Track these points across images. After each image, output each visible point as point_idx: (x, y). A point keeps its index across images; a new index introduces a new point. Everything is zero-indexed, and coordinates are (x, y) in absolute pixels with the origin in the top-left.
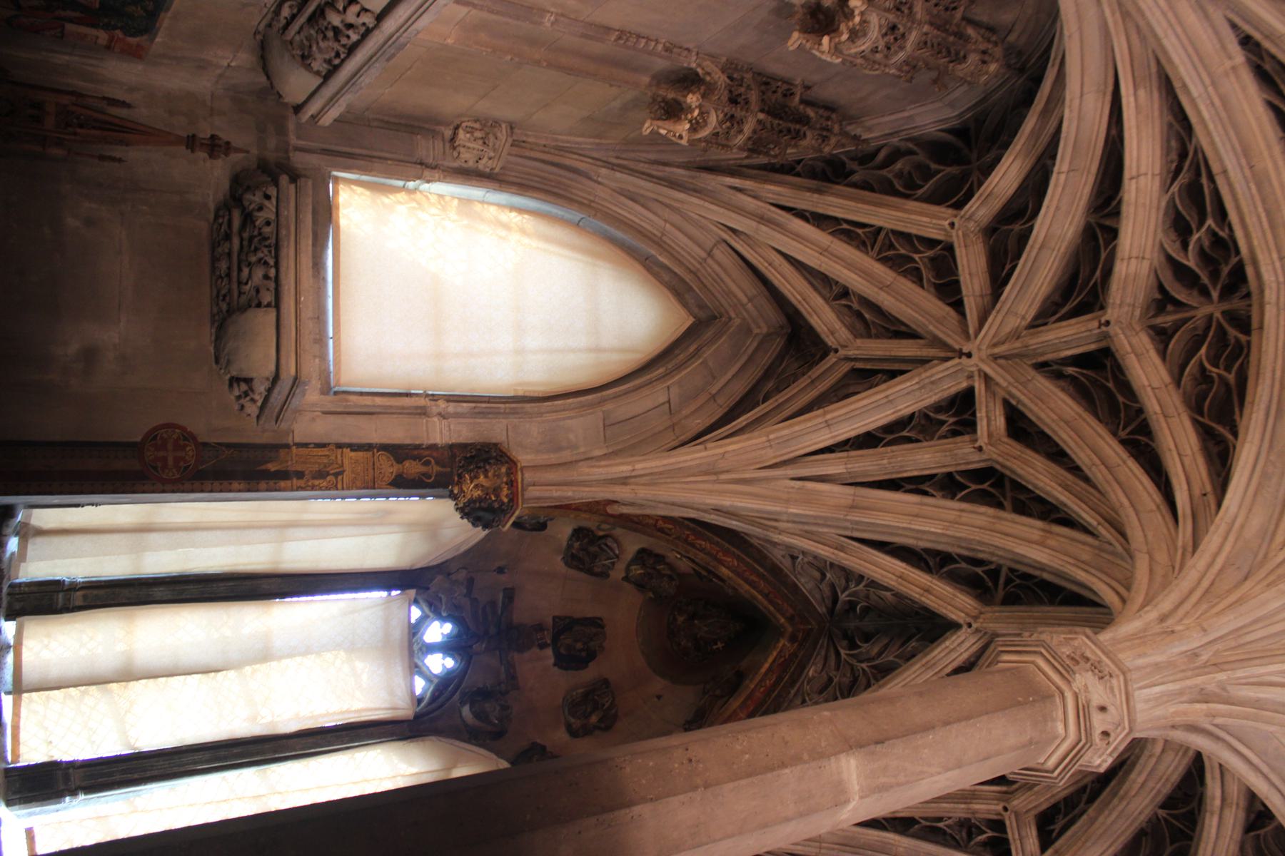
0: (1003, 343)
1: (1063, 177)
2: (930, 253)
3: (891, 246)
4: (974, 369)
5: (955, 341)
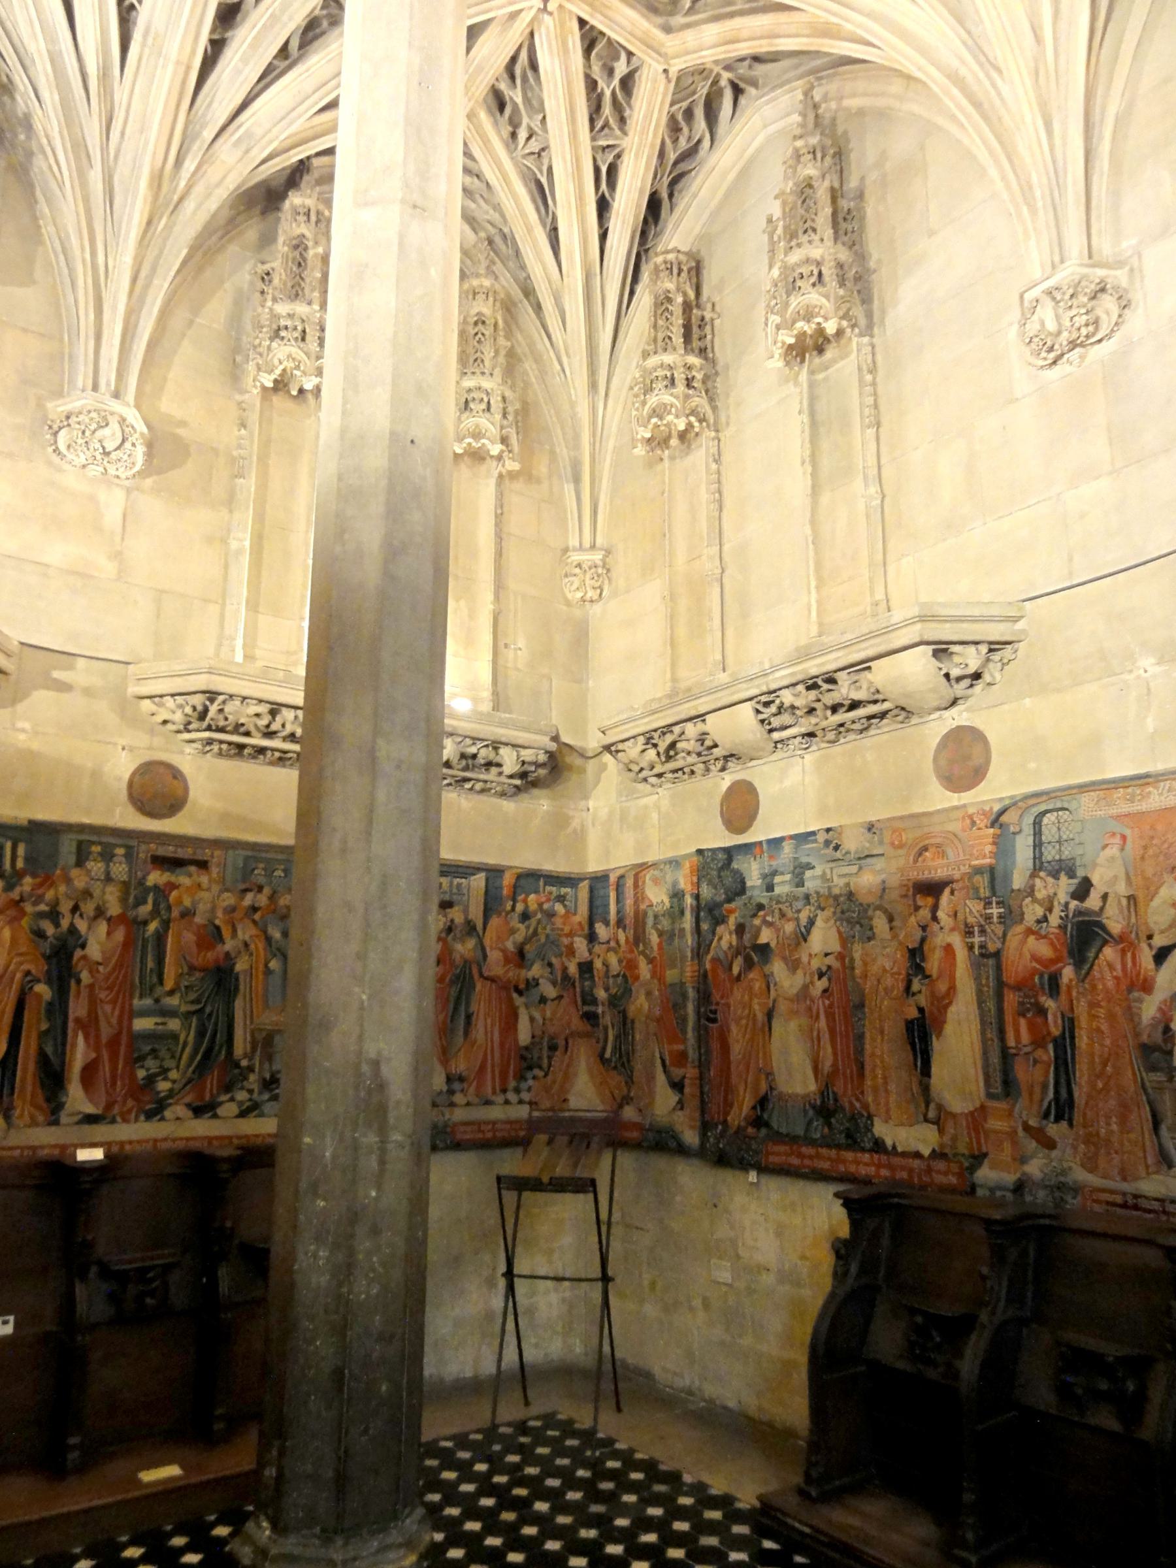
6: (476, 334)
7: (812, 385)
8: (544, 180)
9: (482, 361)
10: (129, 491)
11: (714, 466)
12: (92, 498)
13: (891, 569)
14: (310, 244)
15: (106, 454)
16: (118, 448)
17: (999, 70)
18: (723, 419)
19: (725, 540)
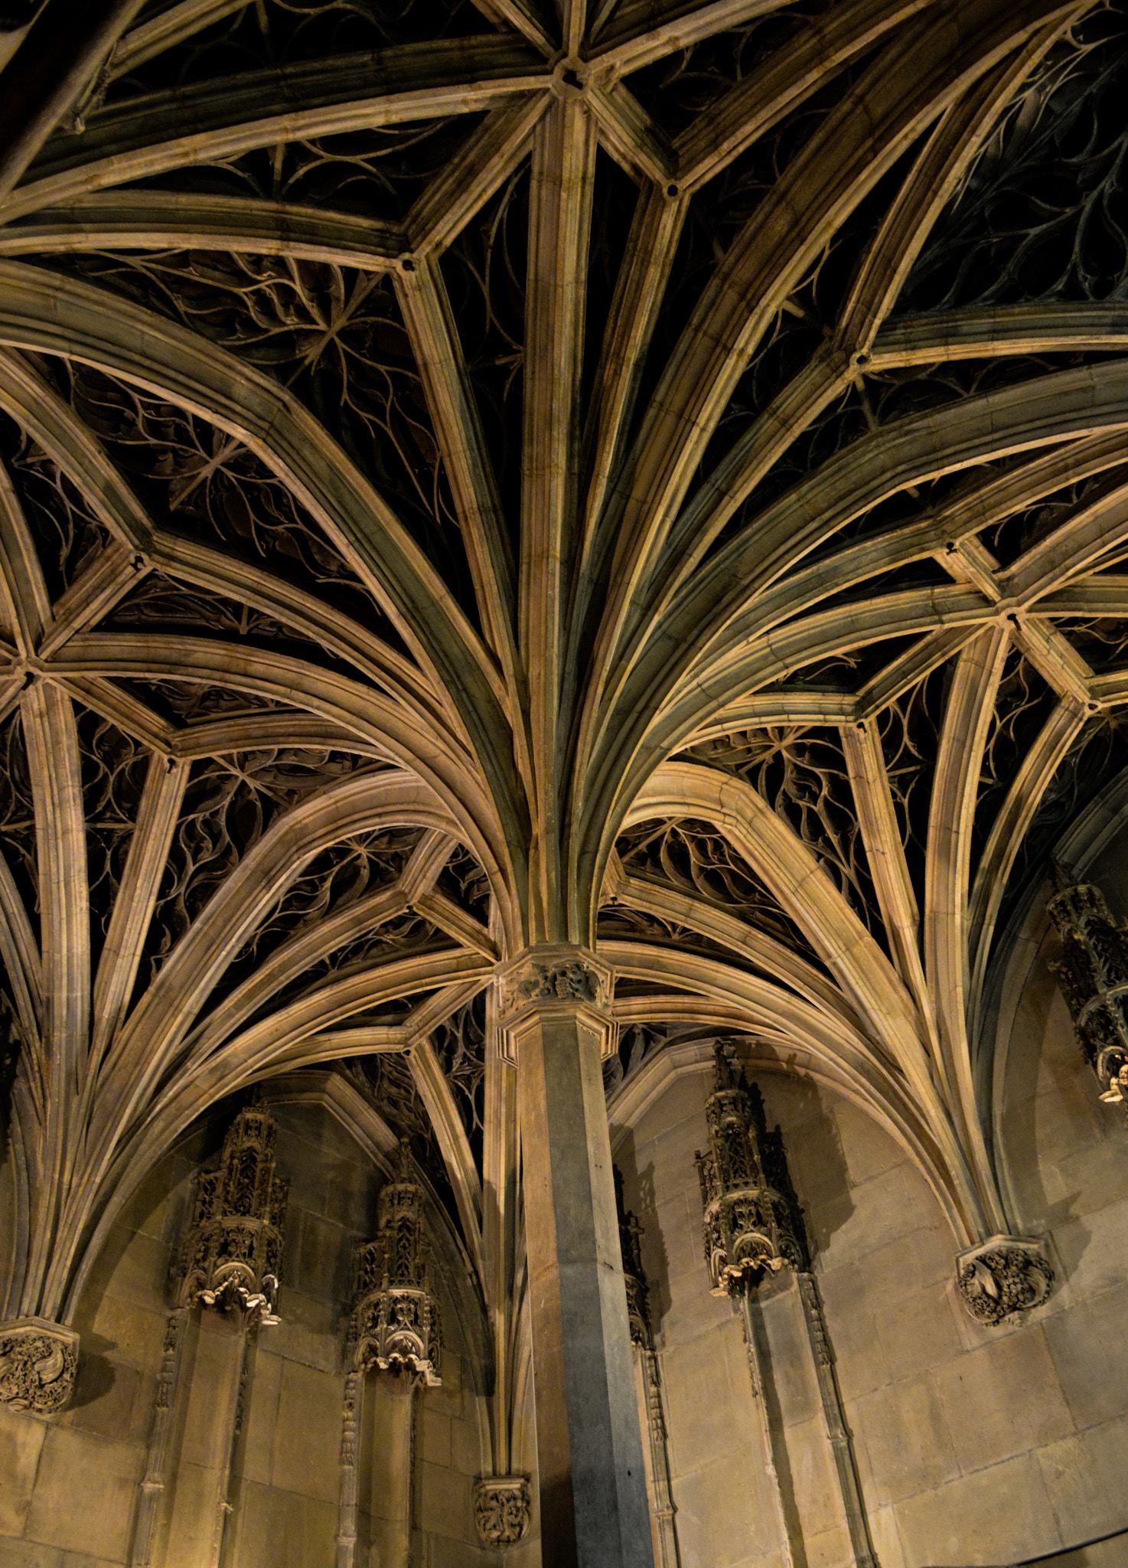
6: (400, 1240)
7: (757, 1315)
8: (472, 1098)
9: (407, 1268)
10: (48, 1426)
11: (653, 1389)
12: (11, 1438)
13: (871, 1519)
14: (259, 1158)
15: (41, 1386)
16: (56, 1380)
17: (901, 1071)
18: (657, 1338)
19: (672, 1475)
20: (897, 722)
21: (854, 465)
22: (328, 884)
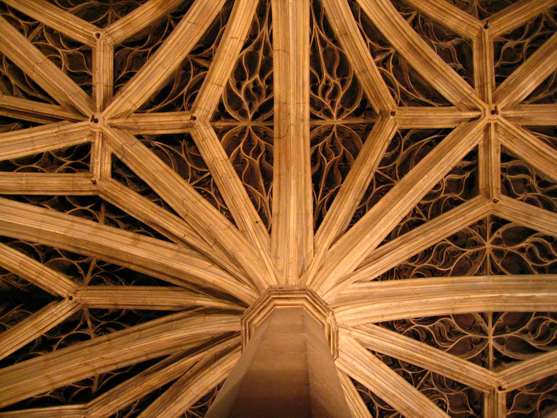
0: (118, 118)
1: (189, 25)
2: (70, 51)
3: (42, 38)
4: (97, 131)
5: (85, 109)
20: (189, 92)
21: (105, 254)
22: (523, 245)
